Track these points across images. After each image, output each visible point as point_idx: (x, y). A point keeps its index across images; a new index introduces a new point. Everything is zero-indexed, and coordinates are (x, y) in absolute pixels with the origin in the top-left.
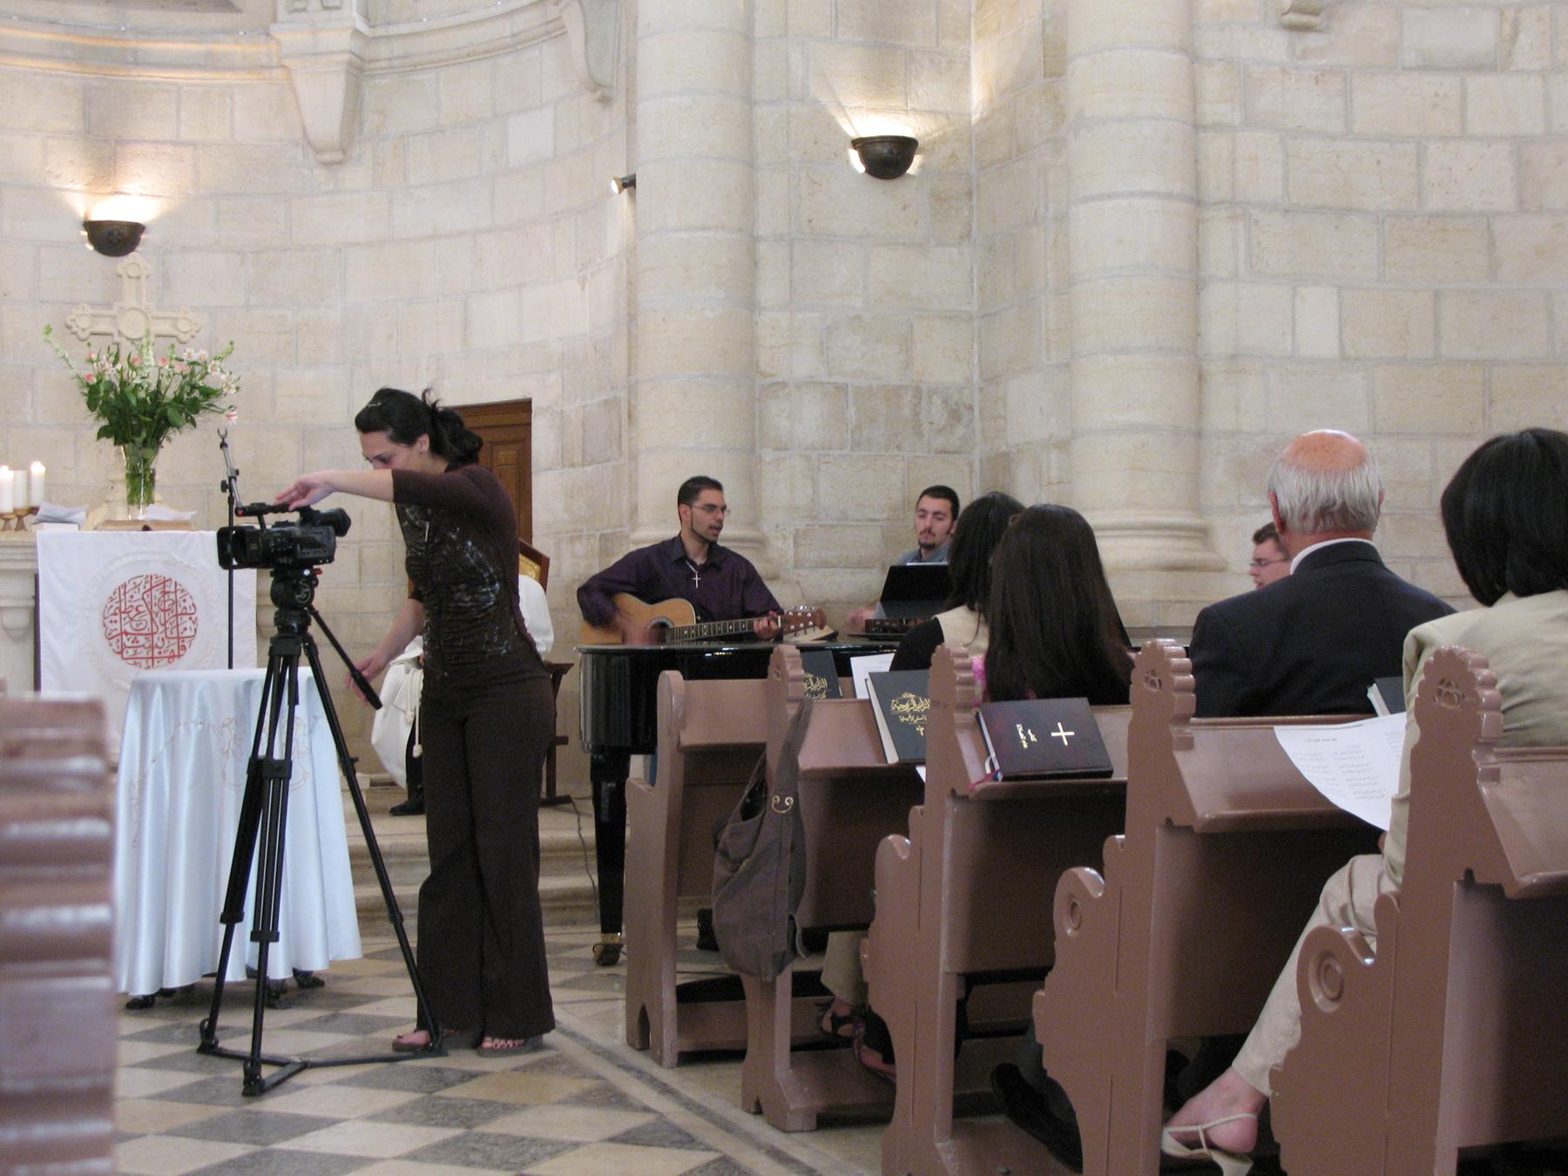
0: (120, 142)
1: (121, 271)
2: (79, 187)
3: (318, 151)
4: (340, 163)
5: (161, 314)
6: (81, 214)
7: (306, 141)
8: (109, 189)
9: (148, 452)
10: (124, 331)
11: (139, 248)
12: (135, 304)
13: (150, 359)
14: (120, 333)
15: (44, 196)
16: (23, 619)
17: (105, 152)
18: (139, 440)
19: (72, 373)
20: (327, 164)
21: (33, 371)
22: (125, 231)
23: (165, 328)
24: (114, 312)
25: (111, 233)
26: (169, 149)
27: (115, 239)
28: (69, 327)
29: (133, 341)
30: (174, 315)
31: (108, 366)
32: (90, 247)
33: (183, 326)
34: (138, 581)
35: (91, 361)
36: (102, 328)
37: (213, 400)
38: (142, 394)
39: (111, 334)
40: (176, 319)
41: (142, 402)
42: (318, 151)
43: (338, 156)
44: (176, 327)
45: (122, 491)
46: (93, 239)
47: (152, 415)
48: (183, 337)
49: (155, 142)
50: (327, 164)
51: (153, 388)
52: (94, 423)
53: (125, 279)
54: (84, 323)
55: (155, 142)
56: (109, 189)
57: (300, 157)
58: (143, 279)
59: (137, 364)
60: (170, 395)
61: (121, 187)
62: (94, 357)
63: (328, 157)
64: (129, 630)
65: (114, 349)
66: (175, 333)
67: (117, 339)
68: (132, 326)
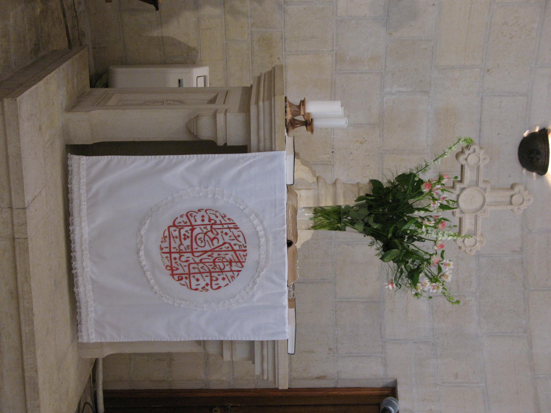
1: (517, 189)
9: (361, 227)
11: (524, 171)
13: (444, 237)
14: (463, 189)
16: (205, 134)
18: (371, 220)
24: (481, 185)
25: (538, 153)
30: (479, 232)
32: (526, 134)
34: (241, 239)
36: (468, 175)
37: (406, 280)
39: (461, 181)
40: (475, 234)
44: (468, 235)
45: (327, 203)
46: (533, 136)
52: (387, 178)
53: (510, 193)
54: (472, 159)
58: (510, 207)
59: (440, 226)
64: (195, 232)
68: (468, 200)
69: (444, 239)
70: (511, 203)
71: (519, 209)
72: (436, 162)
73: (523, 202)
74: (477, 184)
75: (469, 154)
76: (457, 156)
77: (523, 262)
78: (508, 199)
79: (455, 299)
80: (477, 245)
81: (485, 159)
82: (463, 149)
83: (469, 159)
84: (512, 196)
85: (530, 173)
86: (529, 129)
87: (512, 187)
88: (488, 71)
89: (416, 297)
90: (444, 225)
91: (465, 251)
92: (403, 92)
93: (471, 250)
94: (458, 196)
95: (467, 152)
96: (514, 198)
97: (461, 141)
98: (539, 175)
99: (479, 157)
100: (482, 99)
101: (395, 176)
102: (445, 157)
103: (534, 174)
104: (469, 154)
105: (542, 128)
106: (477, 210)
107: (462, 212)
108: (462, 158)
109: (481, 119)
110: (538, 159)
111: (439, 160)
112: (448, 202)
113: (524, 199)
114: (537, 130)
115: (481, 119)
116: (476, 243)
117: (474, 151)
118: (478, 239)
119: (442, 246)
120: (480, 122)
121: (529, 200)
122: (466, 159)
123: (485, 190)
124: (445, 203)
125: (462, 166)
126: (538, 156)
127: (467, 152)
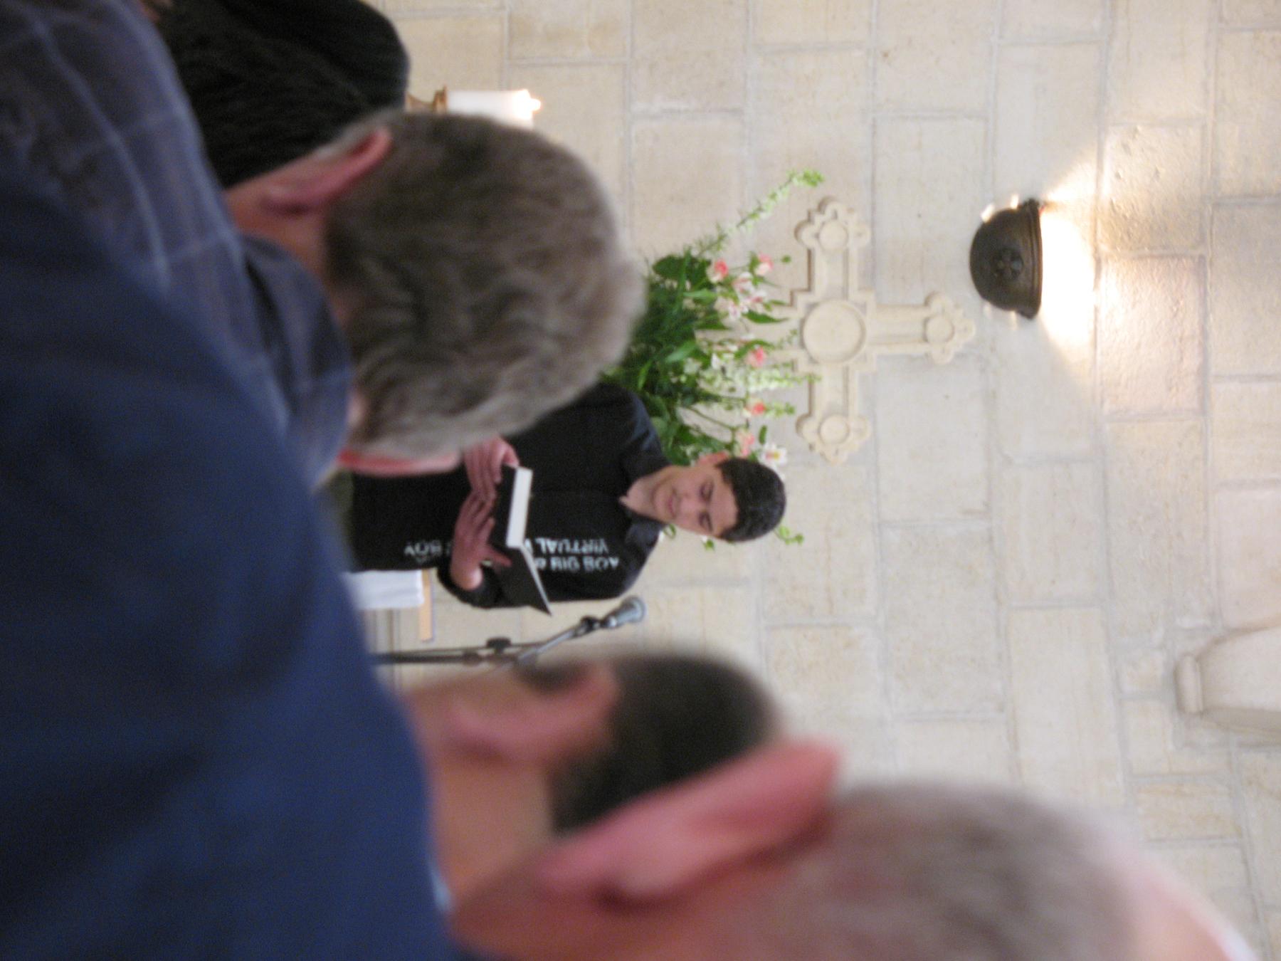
0: (1201, 266)
1: (936, 305)
2: (1107, 190)
3: (1201, 659)
4: (1180, 706)
5: (855, 385)
6: (1051, 196)
7: (1224, 635)
8: (1104, 248)
10: (817, 314)
11: (988, 308)
12: (870, 332)
14: (812, 307)
15: (1085, 122)
17: (1183, 237)
19: (730, 227)
20: (1175, 676)
21: (737, 112)
22: (1022, 281)
23: (827, 392)
24: (855, 295)
25: (1016, 257)
26: (1192, 362)
27: (1005, 261)
28: (821, 207)
29: (799, 332)
30: (856, 407)
31: (745, 304)
32: (987, 215)
33: (832, 429)
35: (754, 263)
38: (691, 367)
39: (809, 289)
40: (845, 413)
41: (678, 368)
42: (1201, 659)
43: (1192, 700)
46: (1003, 220)
47: (651, 386)
48: (809, 427)
49: (1204, 333)
50: (1175, 676)
51: (703, 385)
53: (924, 313)
55: (1204, 333)
56: (1104, 248)
57: (1186, 622)
58: (921, 349)
59: (750, 358)
60: (690, 416)
61: (1110, 271)
62: (763, 269)
63: (1190, 681)
65: (775, 313)
66: (818, 413)
67: (802, 300)
68: (828, 331)
69: (761, 387)
70: (925, 339)
71: (943, 351)
72: (742, 228)
73: (953, 334)
74: (845, 294)
75: (823, 224)
76: (797, 231)
77: (991, 540)
78: (918, 329)
79: (792, 535)
80: (850, 439)
81: (859, 235)
82: (809, 214)
83: (823, 236)
84: (926, 322)
85: (1000, 313)
86: (995, 200)
87: (927, 303)
88: (886, 55)
89: (710, 550)
90: (759, 356)
91: (822, 455)
92: (679, 111)
93: (837, 452)
94: (803, 322)
95: (818, 219)
96: (933, 328)
97: (795, 180)
98: (1025, 320)
99: (845, 229)
100: (874, 126)
101: (653, 261)
102: (763, 216)
103: (1013, 315)
104: (823, 224)
105: (1026, 198)
106: (848, 356)
107: (813, 361)
108: (806, 234)
109: (873, 177)
110: (1015, 273)
111: (750, 223)
112: (767, 306)
113: (953, 328)
114: (1014, 204)
115: (873, 177)
116: (848, 434)
117: (835, 216)
118: (853, 424)
119: (761, 409)
120: (873, 186)
121: (966, 330)
122: (817, 236)
123: (863, 307)
124: (760, 309)
125: (810, 254)
126: (1016, 265)
127: (818, 219)
